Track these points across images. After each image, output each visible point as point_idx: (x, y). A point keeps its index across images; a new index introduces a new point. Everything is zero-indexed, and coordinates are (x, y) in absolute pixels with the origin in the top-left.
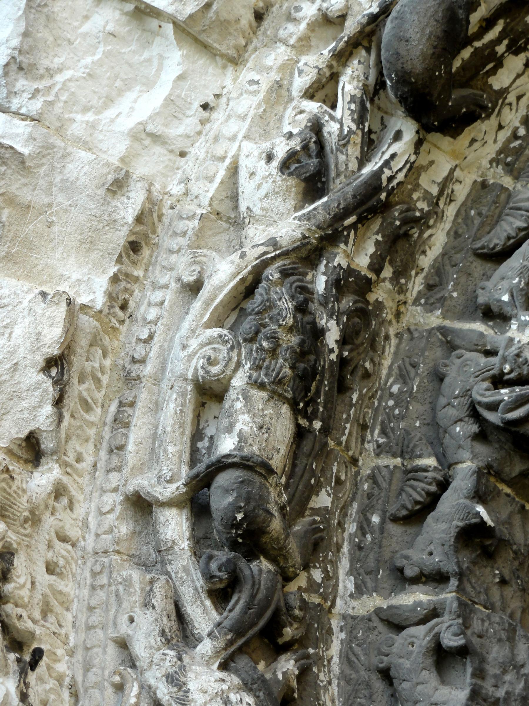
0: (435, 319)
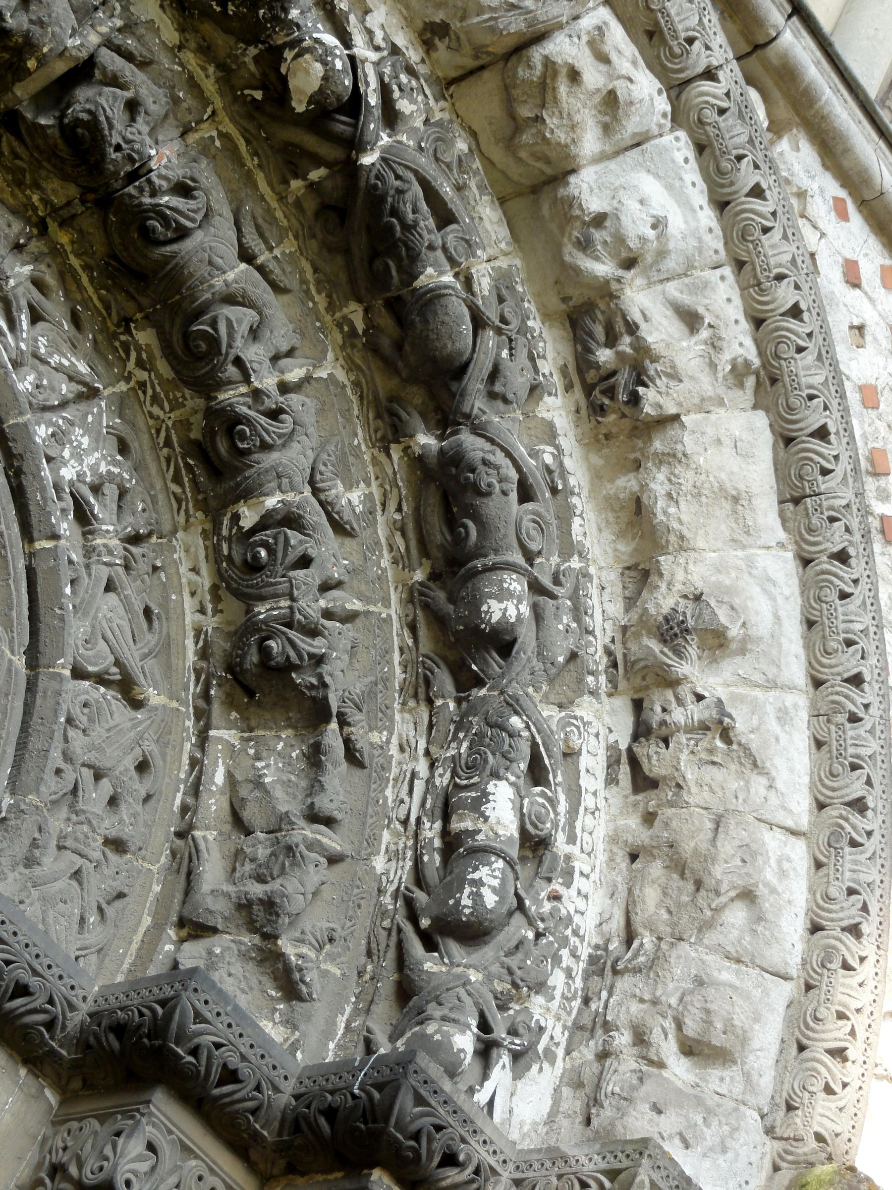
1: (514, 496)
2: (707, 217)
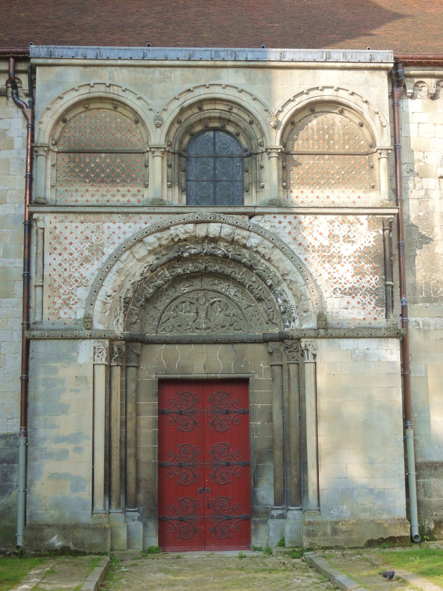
1: (263, 273)
2: (260, 237)
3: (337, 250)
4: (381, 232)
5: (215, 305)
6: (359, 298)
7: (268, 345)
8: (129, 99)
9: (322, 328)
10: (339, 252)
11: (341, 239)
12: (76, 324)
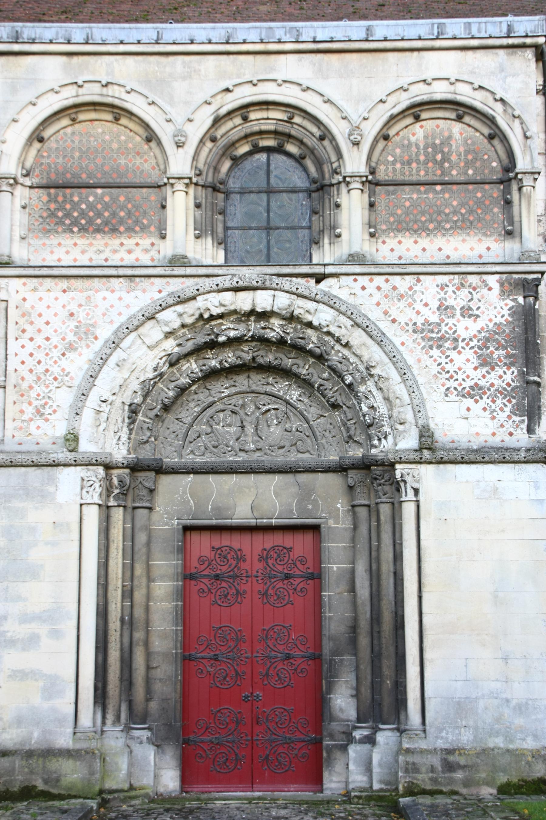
0: (162, 386)
1: (339, 365)
2: (332, 310)
3: (450, 328)
4: (521, 300)
5: (269, 415)
6: (485, 401)
7: (347, 476)
8: (136, 104)
9: (426, 448)
10: (455, 332)
11: (458, 312)
12: (54, 443)
